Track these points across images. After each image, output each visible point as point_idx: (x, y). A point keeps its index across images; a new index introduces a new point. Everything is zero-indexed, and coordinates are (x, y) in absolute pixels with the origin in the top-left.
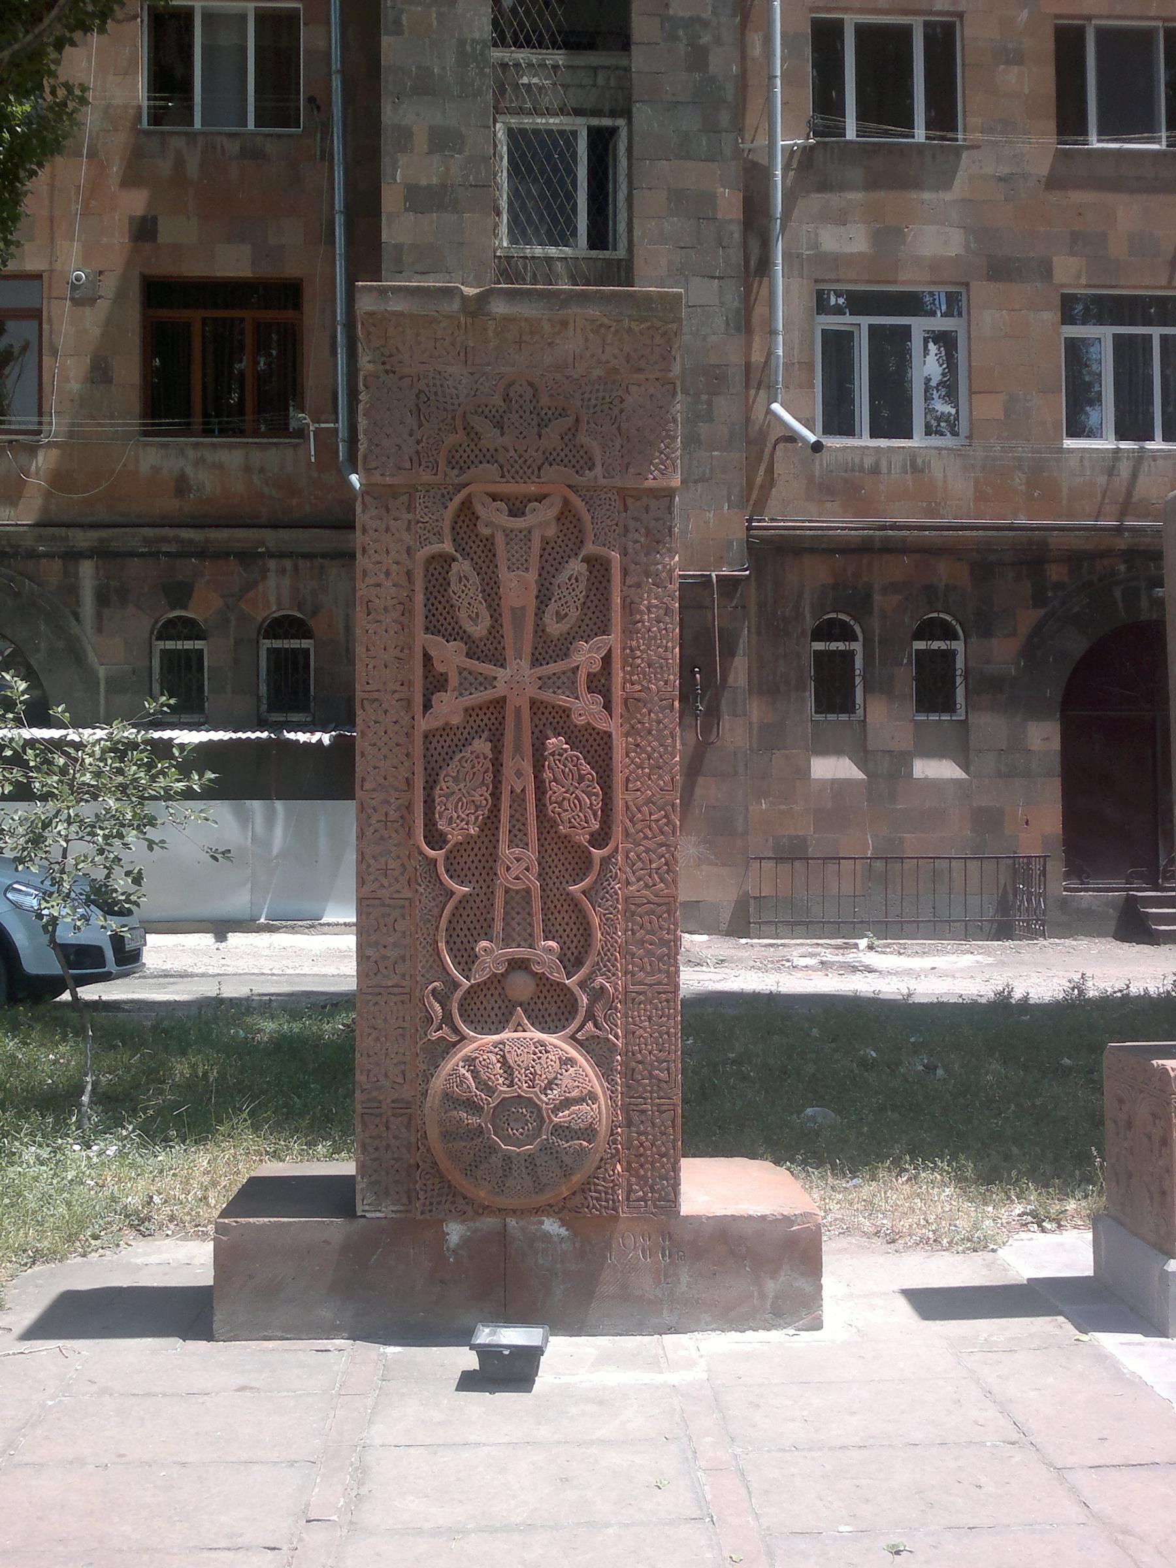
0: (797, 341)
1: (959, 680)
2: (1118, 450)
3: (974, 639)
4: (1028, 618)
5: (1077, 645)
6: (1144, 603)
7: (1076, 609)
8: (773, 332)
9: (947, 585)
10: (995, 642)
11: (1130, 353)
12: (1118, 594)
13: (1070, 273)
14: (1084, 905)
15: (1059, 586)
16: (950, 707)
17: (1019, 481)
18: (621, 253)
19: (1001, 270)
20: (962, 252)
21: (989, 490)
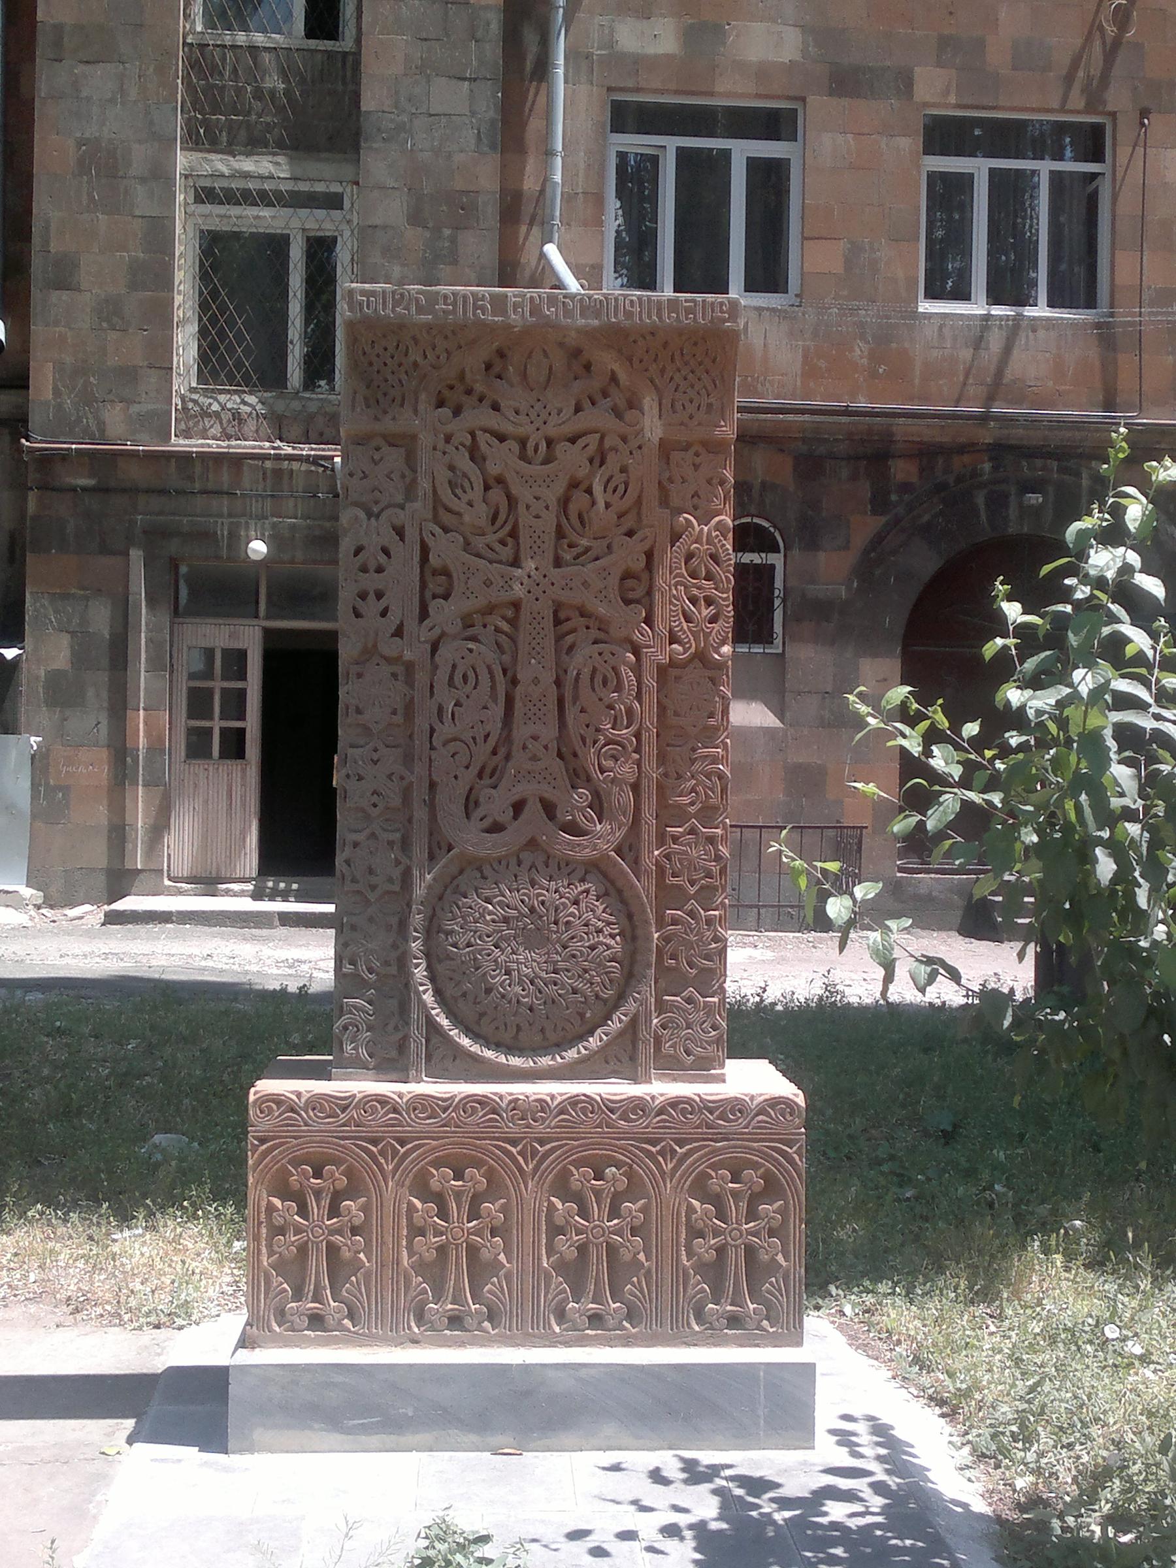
0: (582, 166)
1: (777, 602)
2: (987, 317)
3: (795, 552)
4: (865, 527)
5: (925, 562)
6: (1013, 512)
7: (926, 518)
8: (549, 153)
9: (763, 484)
10: (822, 556)
11: (1010, 193)
12: (980, 500)
13: (936, 90)
14: (923, 891)
15: (905, 487)
16: (768, 639)
17: (860, 352)
18: (346, 44)
19: (846, 82)
20: (797, 57)
21: (822, 364)
